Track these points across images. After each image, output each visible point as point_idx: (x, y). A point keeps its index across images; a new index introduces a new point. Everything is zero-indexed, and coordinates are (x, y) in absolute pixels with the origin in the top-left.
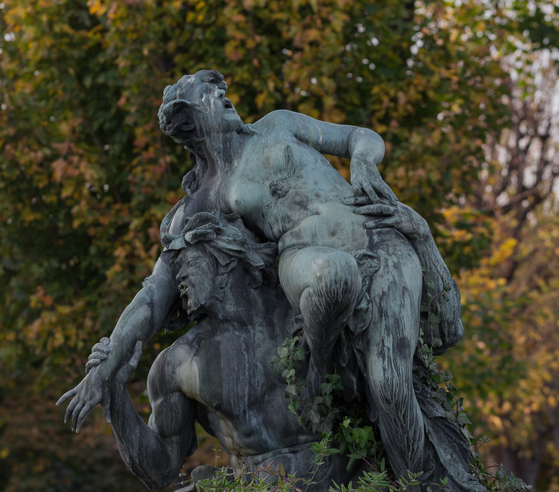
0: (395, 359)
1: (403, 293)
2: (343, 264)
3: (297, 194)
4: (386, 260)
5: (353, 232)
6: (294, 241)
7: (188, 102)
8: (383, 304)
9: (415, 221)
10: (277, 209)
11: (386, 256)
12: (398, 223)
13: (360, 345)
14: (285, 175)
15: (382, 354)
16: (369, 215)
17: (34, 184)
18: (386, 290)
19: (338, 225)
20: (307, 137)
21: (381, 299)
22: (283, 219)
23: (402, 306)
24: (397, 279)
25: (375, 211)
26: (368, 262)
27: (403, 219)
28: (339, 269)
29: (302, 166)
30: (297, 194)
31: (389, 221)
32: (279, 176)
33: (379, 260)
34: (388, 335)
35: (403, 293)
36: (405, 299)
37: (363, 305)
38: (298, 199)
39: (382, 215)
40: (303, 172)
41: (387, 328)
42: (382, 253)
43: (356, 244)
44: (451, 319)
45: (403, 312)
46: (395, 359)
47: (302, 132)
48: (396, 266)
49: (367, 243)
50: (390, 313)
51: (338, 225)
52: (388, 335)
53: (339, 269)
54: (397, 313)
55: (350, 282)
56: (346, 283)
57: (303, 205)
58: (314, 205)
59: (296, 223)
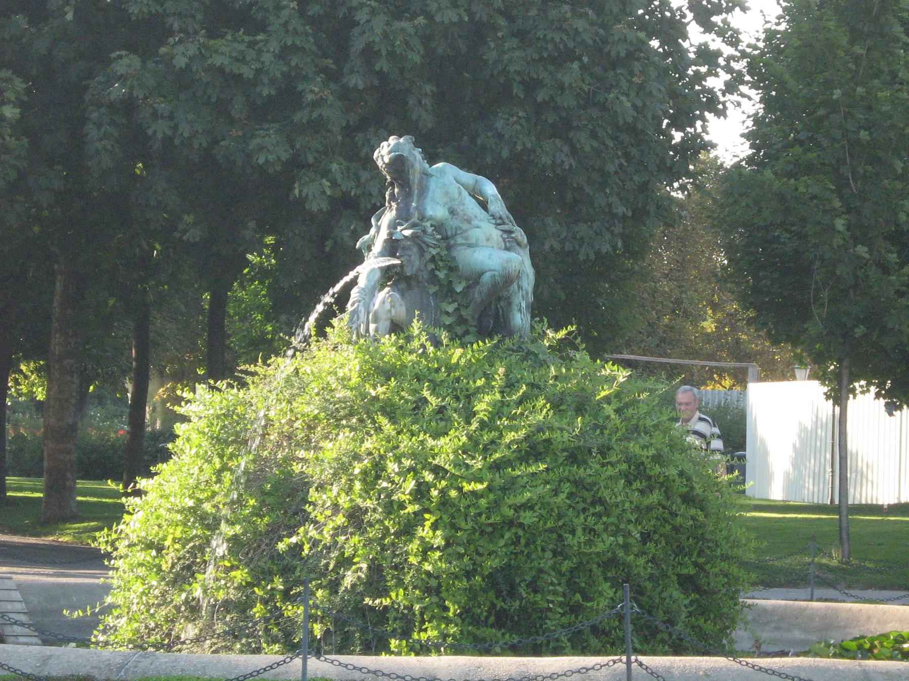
6: (464, 242)
10: (454, 223)
13: (502, 303)
15: (520, 310)
17: (702, 151)
22: (456, 229)
31: (513, 235)
39: (510, 232)
41: (523, 297)
57: (469, 221)
58: (475, 222)
59: (466, 231)
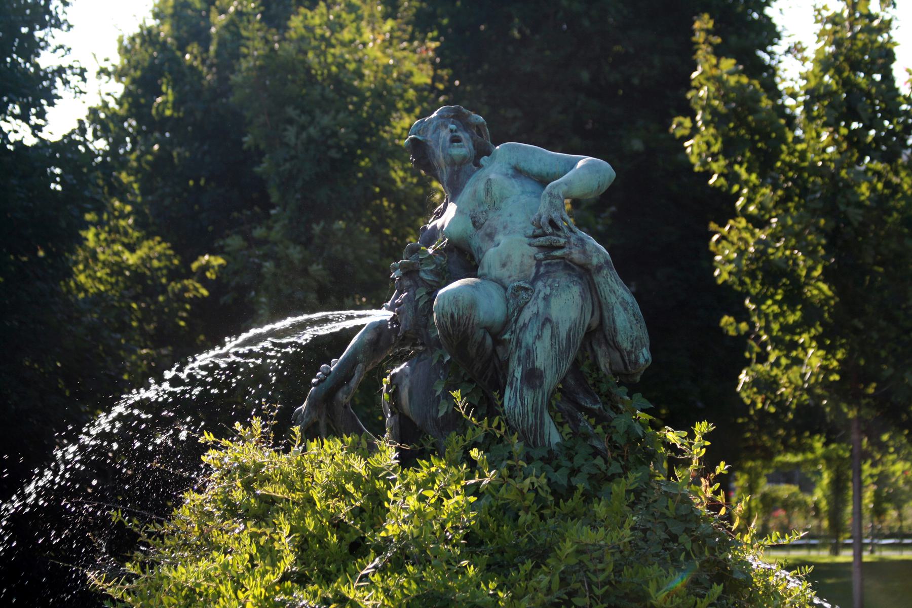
0: (521, 389)
1: (543, 325)
2: (451, 298)
3: (489, 226)
4: (540, 291)
5: (522, 263)
7: (419, 138)
8: (521, 335)
9: (588, 252)
11: (542, 288)
12: (568, 255)
14: (486, 207)
16: (541, 247)
18: (527, 321)
19: (509, 256)
20: (526, 169)
21: (521, 330)
23: (539, 337)
24: (541, 311)
25: (544, 243)
26: (523, 294)
27: (573, 251)
28: (446, 303)
29: (503, 198)
30: (489, 226)
32: (482, 209)
33: (533, 292)
34: (519, 366)
35: (543, 325)
36: (545, 330)
37: (507, 336)
38: (488, 231)
39: (552, 247)
40: (503, 205)
41: (519, 359)
42: (540, 284)
43: (522, 275)
44: (629, 348)
45: (538, 344)
46: (521, 389)
47: (522, 165)
48: (546, 298)
49: (533, 275)
50: (523, 344)
51: (509, 256)
52: (519, 366)
53: (446, 303)
54: (530, 345)
55: (456, 316)
56: (452, 316)
57: (491, 236)
